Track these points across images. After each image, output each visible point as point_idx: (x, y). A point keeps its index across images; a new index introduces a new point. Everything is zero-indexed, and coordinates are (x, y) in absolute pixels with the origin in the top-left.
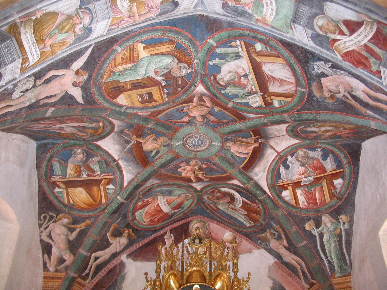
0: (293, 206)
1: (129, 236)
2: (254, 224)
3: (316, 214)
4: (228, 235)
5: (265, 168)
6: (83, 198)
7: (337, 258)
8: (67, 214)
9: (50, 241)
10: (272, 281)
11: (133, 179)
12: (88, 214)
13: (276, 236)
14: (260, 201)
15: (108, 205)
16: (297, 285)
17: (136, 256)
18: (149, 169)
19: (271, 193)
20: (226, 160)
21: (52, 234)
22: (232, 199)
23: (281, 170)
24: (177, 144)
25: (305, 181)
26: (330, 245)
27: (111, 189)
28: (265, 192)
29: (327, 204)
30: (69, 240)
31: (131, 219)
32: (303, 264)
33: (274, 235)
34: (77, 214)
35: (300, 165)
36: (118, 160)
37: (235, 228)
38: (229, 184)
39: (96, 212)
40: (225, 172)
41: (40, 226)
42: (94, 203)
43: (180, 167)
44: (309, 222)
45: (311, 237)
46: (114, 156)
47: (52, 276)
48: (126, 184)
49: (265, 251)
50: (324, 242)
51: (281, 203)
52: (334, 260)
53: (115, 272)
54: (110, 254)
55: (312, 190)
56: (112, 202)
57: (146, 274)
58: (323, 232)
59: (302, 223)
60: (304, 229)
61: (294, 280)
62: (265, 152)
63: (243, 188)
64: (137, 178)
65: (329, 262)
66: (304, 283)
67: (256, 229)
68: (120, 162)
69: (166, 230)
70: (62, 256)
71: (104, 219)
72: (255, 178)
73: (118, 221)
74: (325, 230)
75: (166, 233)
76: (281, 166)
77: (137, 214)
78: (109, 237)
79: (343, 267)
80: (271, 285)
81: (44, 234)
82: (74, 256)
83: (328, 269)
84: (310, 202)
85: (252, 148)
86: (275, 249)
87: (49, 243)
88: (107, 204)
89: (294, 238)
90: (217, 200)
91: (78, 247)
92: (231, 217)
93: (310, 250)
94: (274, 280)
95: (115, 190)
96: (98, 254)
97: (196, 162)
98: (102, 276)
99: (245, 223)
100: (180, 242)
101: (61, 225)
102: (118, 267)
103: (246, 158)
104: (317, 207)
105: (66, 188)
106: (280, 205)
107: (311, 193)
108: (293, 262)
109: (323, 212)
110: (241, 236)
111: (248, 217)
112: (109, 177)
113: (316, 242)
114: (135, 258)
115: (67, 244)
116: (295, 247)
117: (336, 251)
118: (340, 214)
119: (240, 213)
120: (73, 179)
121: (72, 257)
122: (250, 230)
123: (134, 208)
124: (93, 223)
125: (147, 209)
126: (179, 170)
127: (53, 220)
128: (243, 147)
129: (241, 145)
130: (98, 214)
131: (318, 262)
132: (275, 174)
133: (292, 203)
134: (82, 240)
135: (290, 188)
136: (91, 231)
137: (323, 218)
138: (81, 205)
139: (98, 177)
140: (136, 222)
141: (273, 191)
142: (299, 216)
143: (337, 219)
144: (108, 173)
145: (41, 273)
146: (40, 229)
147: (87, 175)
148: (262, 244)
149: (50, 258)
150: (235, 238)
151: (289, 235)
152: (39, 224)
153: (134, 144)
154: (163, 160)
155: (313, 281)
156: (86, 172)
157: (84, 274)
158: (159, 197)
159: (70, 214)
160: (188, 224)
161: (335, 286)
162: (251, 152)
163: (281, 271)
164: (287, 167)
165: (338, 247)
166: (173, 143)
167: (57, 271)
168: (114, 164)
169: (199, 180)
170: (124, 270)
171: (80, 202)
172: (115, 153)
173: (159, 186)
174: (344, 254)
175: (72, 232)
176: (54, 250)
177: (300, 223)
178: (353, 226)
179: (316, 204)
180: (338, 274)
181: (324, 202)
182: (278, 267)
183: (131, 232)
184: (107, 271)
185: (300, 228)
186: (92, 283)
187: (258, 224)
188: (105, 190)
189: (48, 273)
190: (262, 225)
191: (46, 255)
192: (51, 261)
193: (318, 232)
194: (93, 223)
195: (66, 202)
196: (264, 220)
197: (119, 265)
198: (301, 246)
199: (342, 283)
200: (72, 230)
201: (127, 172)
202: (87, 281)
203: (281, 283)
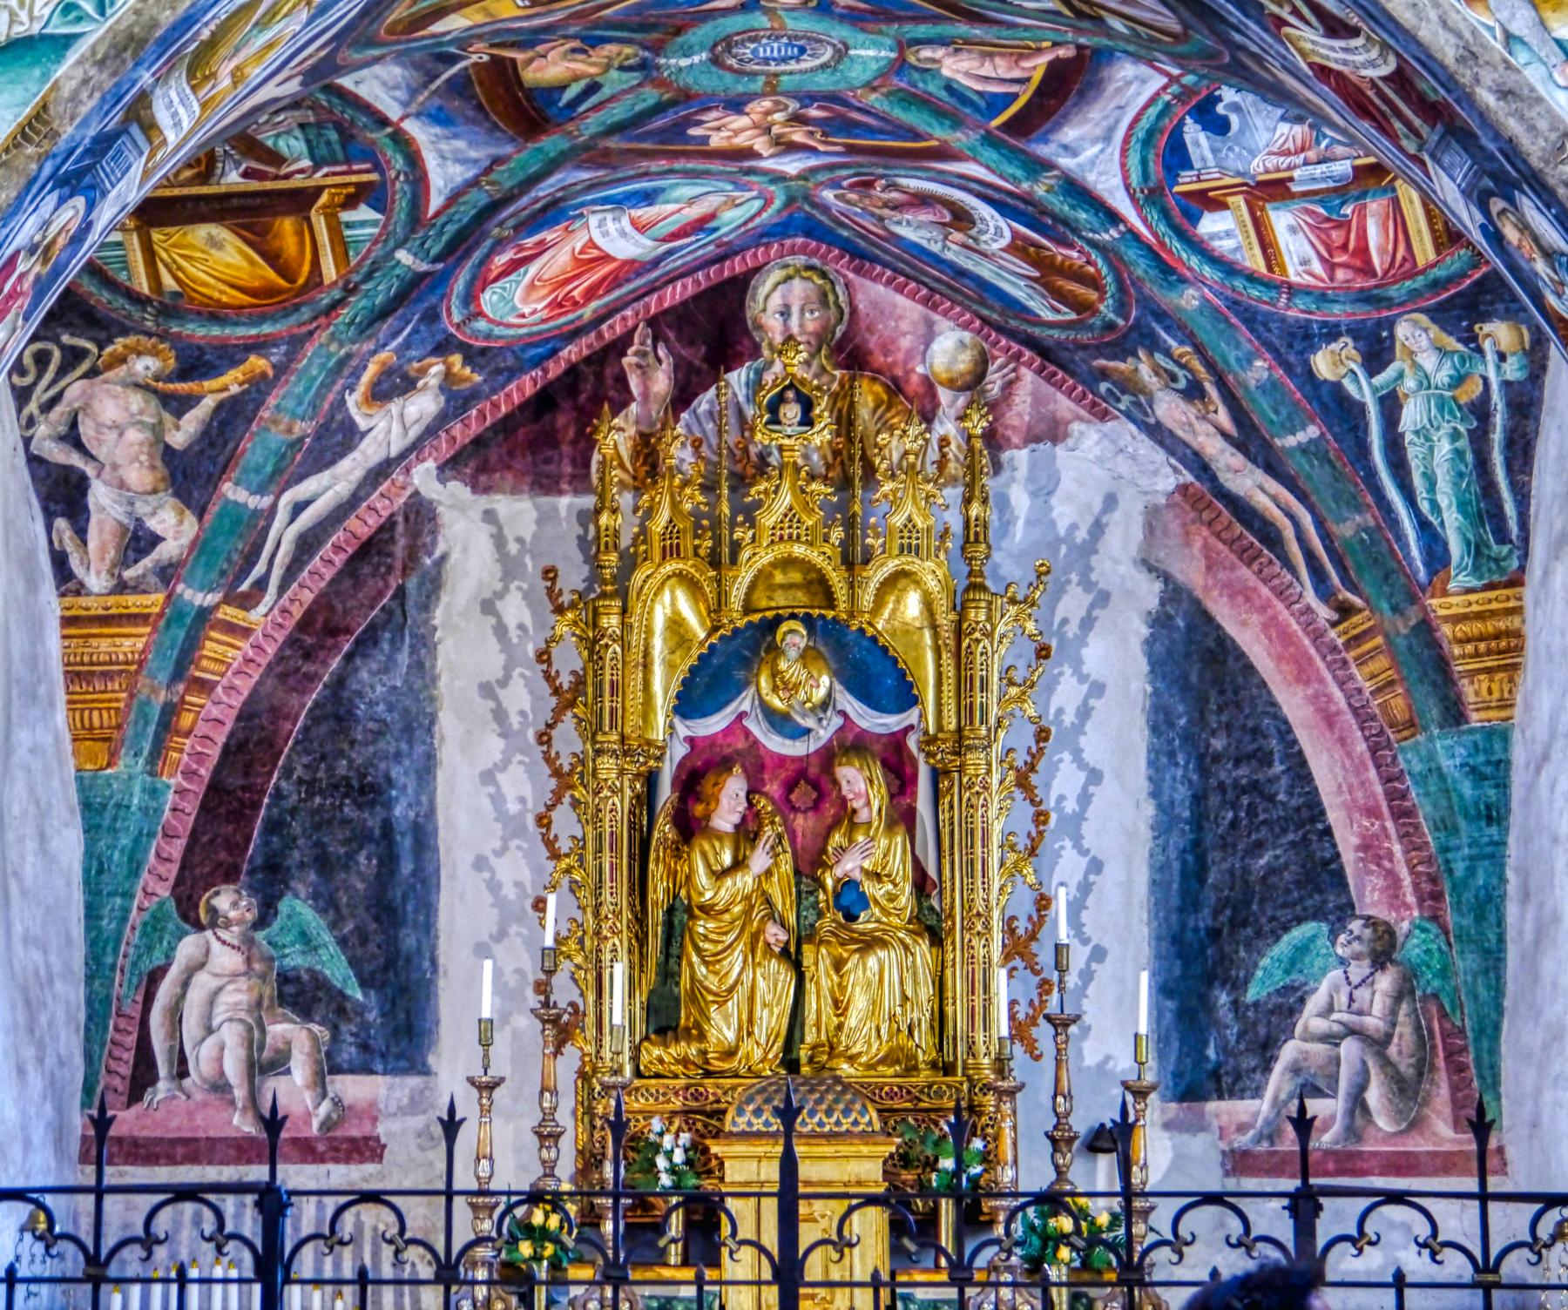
0: (1252, 278)
2: (1073, 316)
3: (1363, 313)
4: (948, 349)
5: (1111, 130)
6: (228, 265)
7: (1462, 507)
8: (149, 335)
9: (76, 460)
10: (1158, 586)
11: (474, 183)
12: (253, 332)
13: (1182, 384)
14: (1094, 244)
15: (350, 290)
16: (1280, 606)
17: (484, 468)
18: (552, 144)
19: (1144, 221)
20: (923, 102)
21: (81, 429)
22: (961, 219)
23: (1188, 138)
24: (684, 62)
25: (1304, 177)
26: (1431, 449)
27: (363, 224)
28: (1114, 217)
29: (1422, 272)
30: (167, 447)
31: (457, 318)
32: (1307, 519)
33: (1174, 378)
34: (201, 332)
35: (1283, 118)
36: (402, 119)
37: (985, 312)
38: (942, 172)
39: (293, 320)
40: (917, 136)
41: (22, 396)
42: (282, 282)
43: (699, 123)
44: (1334, 346)
45: (1339, 409)
46: (380, 107)
47: (101, 612)
48: (436, 202)
49: (1133, 428)
50: (1402, 435)
51: (1194, 261)
52: (1445, 515)
53: (390, 555)
54: (358, 474)
55: (1348, 210)
56: (369, 276)
57: (550, 574)
58: (1401, 391)
59: (1298, 347)
61: (1265, 581)
62: (1105, 73)
63: (1010, 193)
64: (493, 177)
65: (1423, 525)
66: (1310, 597)
67: (1084, 337)
68: (412, 127)
69: (630, 323)
70: (139, 521)
71: (333, 347)
72: (1065, 162)
73: (400, 339)
74: (1410, 383)
75: (625, 341)
76: (1188, 120)
77: (489, 299)
78: (353, 411)
79: (1489, 547)
80: (1153, 603)
81: (42, 430)
82: (201, 513)
83: (1415, 552)
84: (1338, 259)
85: (1042, 61)
86: (1180, 433)
87: (69, 469)
88: (348, 282)
89: (1263, 410)
90: (886, 212)
91: (213, 481)
92: (961, 273)
93: (1334, 467)
95: (385, 226)
97: (777, 103)
98: (328, 578)
99: (1031, 304)
100: (706, 389)
101: (125, 385)
102: (400, 528)
103: (1015, 96)
104: (1372, 282)
105: (138, 229)
106: (1190, 269)
107: (1344, 225)
108: (1262, 501)
109: (1401, 304)
110: (1015, 347)
111: (1046, 286)
112: (354, 178)
113: (1366, 431)
114: (483, 478)
115: (159, 463)
116: (1267, 445)
117: (1461, 475)
118: (1485, 317)
119: (1001, 267)
120: (176, 192)
121: (190, 526)
122: (1056, 333)
123: (474, 278)
124: (281, 370)
125: (533, 269)
126: (693, 132)
127: (85, 366)
128: (998, 60)
129: (991, 55)
130: (304, 330)
131: (1372, 523)
133: (1248, 264)
134: (231, 445)
135: (1238, 201)
136: (272, 401)
137: (1402, 330)
138: (216, 295)
139: (298, 182)
140: (481, 325)
141: (1154, 216)
142: (1283, 320)
143: (1470, 339)
144: (348, 162)
145: (52, 605)
146: (19, 411)
147: (246, 175)
148: (1118, 400)
149: (81, 533)
150: (983, 362)
151: (1239, 393)
152: (13, 387)
153: (475, 64)
154: (618, 112)
155: (1349, 595)
156: (238, 164)
157: (245, 587)
158: (593, 221)
159: (163, 336)
160: (739, 287)
161: (1446, 629)
162: (1037, 76)
163: (1205, 532)
164: (1219, 127)
165: (1469, 457)
166: (663, 61)
167: (121, 587)
168: (380, 136)
170: (434, 543)
171: (212, 281)
172: (383, 96)
173: (592, 186)
174: (1498, 492)
175: (179, 414)
176: (100, 496)
177: (1290, 346)
178: (1544, 368)
179: (1367, 270)
180: (1460, 579)
181: (1407, 266)
182: (1193, 515)
183: (457, 368)
184: (350, 551)
185: (1288, 368)
186: (284, 611)
187: (1096, 321)
189: (83, 601)
190: (1110, 326)
191: (61, 523)
192: (93, 544)
193: (1375, 390)
194: (281, 370)
195: (143, 286)
196: (1122, 308)
197: (407, 519)
198: (1292, 449)
199: (1480, 616)
200: (178, 405)
201: (443, 158)
202: (262, 609)
203: (1199, 593)
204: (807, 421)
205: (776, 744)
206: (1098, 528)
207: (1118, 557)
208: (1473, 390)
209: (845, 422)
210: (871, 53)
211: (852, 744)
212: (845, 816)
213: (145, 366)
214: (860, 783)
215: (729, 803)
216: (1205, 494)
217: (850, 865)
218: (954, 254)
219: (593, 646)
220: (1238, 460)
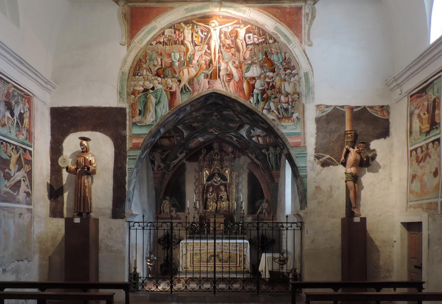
1: (186, 153)
22: (232, 138)
25: (262, 135)
28: (245, 138)
45: (264, 155)
57: (195, 169)
60: (262, 152)
75: (202, 148)
77: (190, 145)
94: (249, 170)
96: (174, 161)
132: (249, 132)
137: (270, 148)
143: (276, 149)
150: (233, 150)
167: (158, 170)
169: (217, 132)
176: (156, 163)
188: (176, 139)
200: (163, 155)
204: (218, 156)
205: (215, 184)
206: (244, 164)
207: (245, 167)
208: (276, 153)
209: (221, 156)
210: (223, 124)
211: (222, 184)
212: (221, 191)
213: (160, 151)
214: (222, 188)
215: (211, 190)
216: (253, 162)
217: (221, 195)
218: (231, 141)
219: (199, 175)
220: (255, 159)
